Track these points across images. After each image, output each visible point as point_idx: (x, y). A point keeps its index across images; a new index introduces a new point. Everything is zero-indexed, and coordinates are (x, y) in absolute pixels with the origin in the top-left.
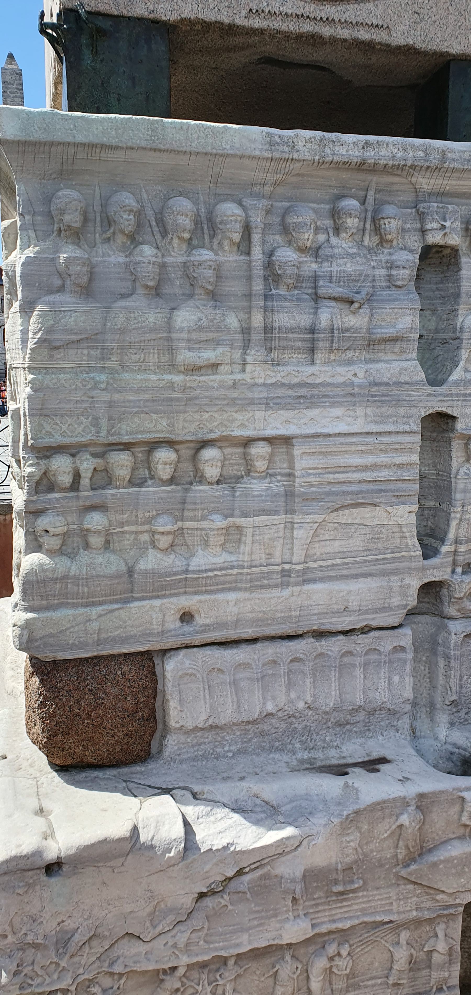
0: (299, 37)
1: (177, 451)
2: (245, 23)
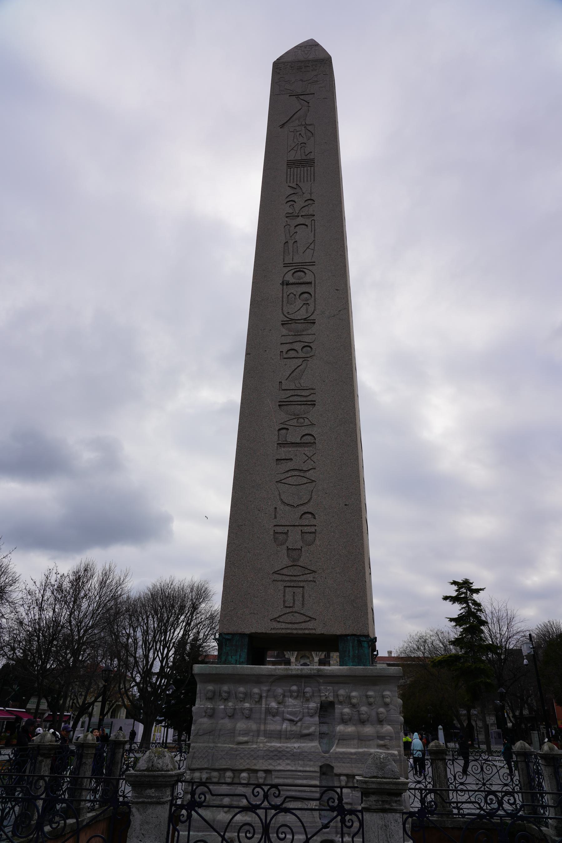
0: (287, 634)
1: (234, 773)
2: (270, 632)
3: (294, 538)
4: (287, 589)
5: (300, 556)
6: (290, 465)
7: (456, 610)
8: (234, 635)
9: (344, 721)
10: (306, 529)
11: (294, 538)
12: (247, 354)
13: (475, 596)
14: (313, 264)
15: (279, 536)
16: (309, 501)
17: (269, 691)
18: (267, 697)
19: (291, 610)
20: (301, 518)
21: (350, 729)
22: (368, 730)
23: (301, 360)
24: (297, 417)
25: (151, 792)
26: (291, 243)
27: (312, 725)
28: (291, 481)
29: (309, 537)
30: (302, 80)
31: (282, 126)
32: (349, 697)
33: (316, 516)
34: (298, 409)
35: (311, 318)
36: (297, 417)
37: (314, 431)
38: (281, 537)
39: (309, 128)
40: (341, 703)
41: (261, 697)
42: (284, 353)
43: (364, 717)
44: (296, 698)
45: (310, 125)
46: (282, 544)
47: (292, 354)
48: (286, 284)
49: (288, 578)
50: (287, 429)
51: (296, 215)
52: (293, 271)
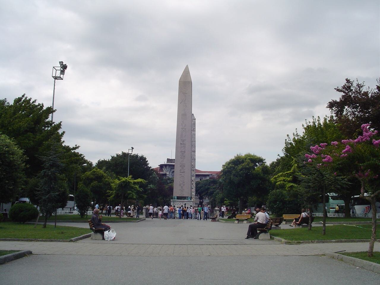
3: (182, 185)
11: (182, 185)
14: (185, 140)
15: (180, 185)
31: (181, 103)
37: (185, 171)
47: (182, 158)
48: (181, 144)
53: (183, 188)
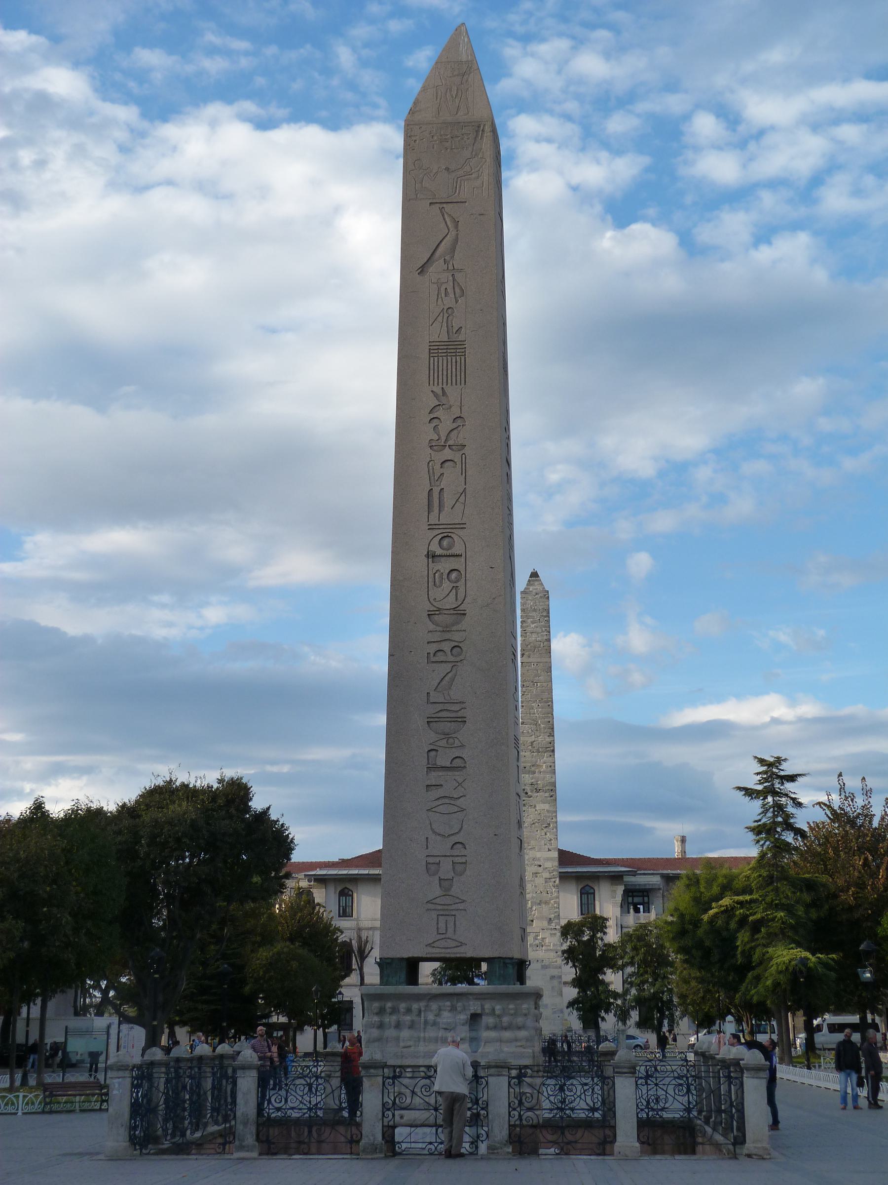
4: (440, 917)
5: (451, 886)
6: (440, 792)
7: (753, 809)
8: (392, 959)
9: (488, 1028)
10: (457, 860)
12: (391, 655)
13: (789, 786)
14: (462, 526)
15: (431, 867)
16: (460, 830)
17: (427, 1006)
18: (425, 1011)
19: (443, 936)
20: (452, 848)
21: (493, 1034)
22: (507, 1035)
23: (450, 665)
24: (447, 735)
25: (372, 1071)
26: (436, 491)
27: (464, 1032)
28: (441, 809)
29: (459, 868)
30: (447, 169)
31: (422, 270)
32: (493, 1010)
33: (467, 847)
34: (447, 727)
35: (461, 608)
36: (447, 735)
38: (433, 868)
39: (458, 276)
40: (487, 1014)
41: (420, 1011)
42: (432, 655)
43: (505, 1025)
44: (450, 1011)
45: (460, 270)
46: (434, 875)
47: (440, 657)
48: (432, 556)
49: (440, 907)
50: (437, 751)
51: (443, 443)
52: (440, 537)
53: (455, 890)
